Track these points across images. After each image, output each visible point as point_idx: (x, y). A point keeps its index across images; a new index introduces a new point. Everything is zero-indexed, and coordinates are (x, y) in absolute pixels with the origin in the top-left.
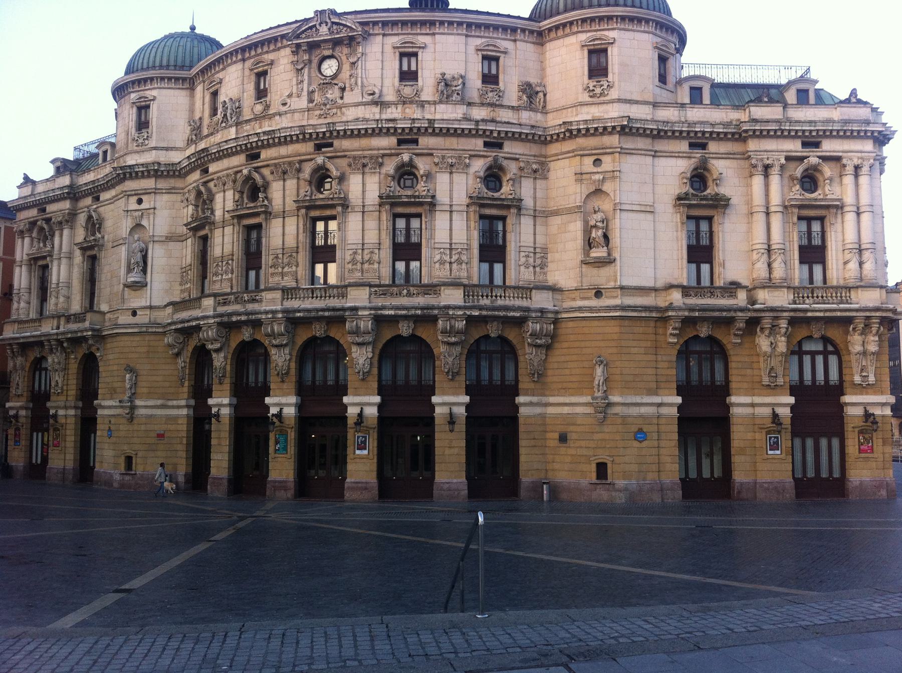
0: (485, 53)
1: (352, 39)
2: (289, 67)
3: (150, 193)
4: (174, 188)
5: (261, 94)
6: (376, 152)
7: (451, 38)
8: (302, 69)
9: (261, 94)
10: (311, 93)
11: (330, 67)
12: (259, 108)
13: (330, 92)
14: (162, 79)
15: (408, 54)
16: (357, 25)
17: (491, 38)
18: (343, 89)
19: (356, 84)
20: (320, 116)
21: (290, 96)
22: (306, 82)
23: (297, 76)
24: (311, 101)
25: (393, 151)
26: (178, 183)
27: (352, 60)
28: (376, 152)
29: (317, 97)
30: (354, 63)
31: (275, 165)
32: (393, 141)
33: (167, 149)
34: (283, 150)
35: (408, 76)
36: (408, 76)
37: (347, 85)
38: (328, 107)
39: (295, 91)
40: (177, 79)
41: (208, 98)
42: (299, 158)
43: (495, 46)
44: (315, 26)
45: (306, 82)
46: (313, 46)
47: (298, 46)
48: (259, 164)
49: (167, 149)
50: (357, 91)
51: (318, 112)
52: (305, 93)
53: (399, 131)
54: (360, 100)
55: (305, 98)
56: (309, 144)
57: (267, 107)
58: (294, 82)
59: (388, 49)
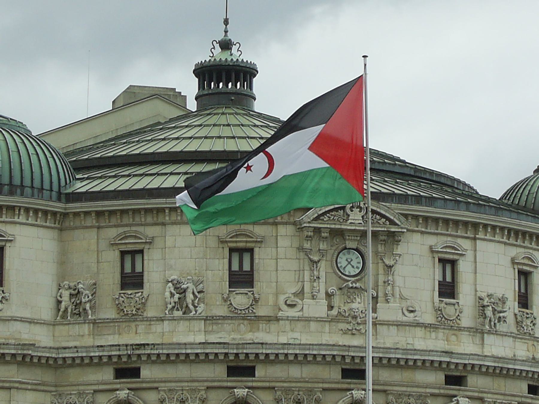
0: (521, 267)
1: (392, 235)
2: (292, 253)
3: (10, 388)
4: (43, 384)
5: (241, 279)
6: (423, 390)
7: (492, 246)
8: (319, 261)
9: (241, 279)
10: (329, 296)
11: (350, 264)
12: (240, 299)
13: (358, 300)
14: (27, 210)
15: (449, 263)
16: (403, 219)
17: (525, 247)
18: (375, 299)
19: (393, 295)
20: (345, 332)
21: (300, 294)
22: (323, 279)
23: (312, 270)
24: (331, 308)
25: (442, 391)
26: (48, 376)
27: (387, 262)
28: (423, 390)
29: (337, 301)
30: (391, 267)
31: (287, 391)
32: (441, 377)
33: (31, 322)
34: (295, 371)
35: (448, 290)
36: (448, 290)
37: (381, 294)
38: (359, 320)
39: (307, 289)
40: (45, 213)
41: (112, 256)
42: (321, 385)
43: (529, 259)
44: (343, 208)
45: (323, 279)
46: (338, 234)
47: (317, 230)
48: (255, 384)
49: (31, 322)
50: (394, 304)
51: (343, 326)
52: (322, 294)
53: (453, 367)
54: (400, 318)
55: (324, 302)
56: (333, 368)
57: (256, 300)
58: (307, 278)
59: (425, 250)
